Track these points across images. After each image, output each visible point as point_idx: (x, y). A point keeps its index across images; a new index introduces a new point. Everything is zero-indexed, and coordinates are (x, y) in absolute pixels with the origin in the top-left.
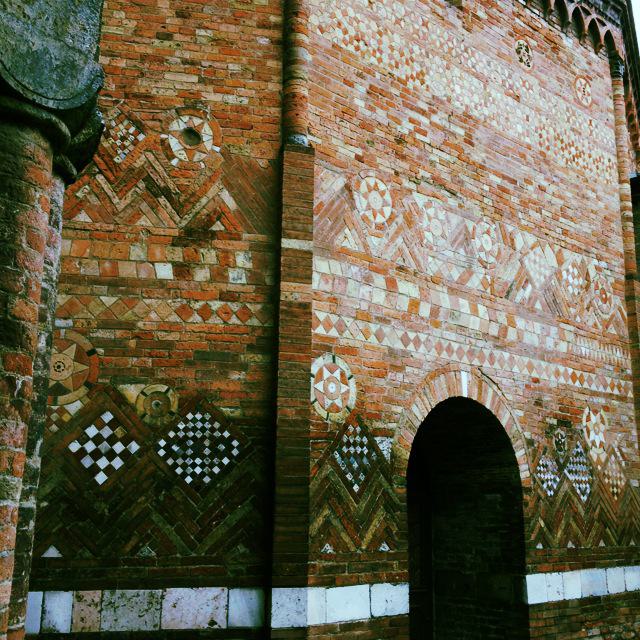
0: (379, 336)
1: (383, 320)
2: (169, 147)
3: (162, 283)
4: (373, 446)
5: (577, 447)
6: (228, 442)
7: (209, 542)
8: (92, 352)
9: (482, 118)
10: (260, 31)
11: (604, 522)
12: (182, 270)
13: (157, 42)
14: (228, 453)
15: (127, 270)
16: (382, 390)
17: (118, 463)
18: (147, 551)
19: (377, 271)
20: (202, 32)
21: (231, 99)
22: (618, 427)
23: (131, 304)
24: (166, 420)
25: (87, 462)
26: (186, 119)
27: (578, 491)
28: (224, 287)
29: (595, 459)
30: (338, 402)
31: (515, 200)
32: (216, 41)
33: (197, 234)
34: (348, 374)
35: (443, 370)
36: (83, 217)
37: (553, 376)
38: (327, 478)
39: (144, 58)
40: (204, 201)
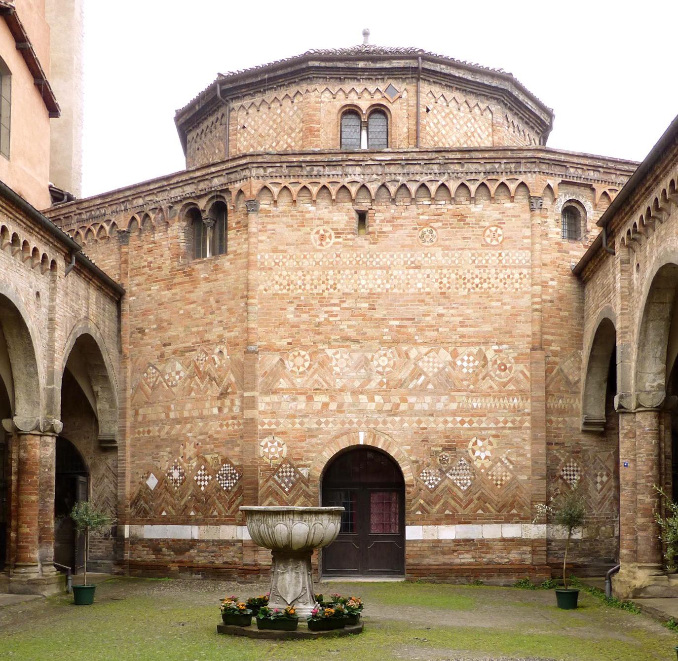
0: (301, 424)
1: (305, 416)
4: (296, 472)
5: (461, 461)
7: (231, 510)
9: (385, 291)
11: (483, 499)
12: (220, 410)
13: (210, 316)
15: (205, 412)
16: (303, 448)
17: (206, 483)
18: (215, 513)
19: (301, 394)
20: (223, 307)
21: (233, 334)
22: (509, 446)
23: (206, 424)
25: (199, 483)
26: (219, 347)
28: (233, 414)
29: (479, 465)
30: (277, 455)
31: (411, 330)
33: (223, 395)
34: (282, 443)
35: (347, 433)
36: (193, 394)
37: (437, 425)
38: (270, 486)
39: (207, 324)
40: (225, 380)
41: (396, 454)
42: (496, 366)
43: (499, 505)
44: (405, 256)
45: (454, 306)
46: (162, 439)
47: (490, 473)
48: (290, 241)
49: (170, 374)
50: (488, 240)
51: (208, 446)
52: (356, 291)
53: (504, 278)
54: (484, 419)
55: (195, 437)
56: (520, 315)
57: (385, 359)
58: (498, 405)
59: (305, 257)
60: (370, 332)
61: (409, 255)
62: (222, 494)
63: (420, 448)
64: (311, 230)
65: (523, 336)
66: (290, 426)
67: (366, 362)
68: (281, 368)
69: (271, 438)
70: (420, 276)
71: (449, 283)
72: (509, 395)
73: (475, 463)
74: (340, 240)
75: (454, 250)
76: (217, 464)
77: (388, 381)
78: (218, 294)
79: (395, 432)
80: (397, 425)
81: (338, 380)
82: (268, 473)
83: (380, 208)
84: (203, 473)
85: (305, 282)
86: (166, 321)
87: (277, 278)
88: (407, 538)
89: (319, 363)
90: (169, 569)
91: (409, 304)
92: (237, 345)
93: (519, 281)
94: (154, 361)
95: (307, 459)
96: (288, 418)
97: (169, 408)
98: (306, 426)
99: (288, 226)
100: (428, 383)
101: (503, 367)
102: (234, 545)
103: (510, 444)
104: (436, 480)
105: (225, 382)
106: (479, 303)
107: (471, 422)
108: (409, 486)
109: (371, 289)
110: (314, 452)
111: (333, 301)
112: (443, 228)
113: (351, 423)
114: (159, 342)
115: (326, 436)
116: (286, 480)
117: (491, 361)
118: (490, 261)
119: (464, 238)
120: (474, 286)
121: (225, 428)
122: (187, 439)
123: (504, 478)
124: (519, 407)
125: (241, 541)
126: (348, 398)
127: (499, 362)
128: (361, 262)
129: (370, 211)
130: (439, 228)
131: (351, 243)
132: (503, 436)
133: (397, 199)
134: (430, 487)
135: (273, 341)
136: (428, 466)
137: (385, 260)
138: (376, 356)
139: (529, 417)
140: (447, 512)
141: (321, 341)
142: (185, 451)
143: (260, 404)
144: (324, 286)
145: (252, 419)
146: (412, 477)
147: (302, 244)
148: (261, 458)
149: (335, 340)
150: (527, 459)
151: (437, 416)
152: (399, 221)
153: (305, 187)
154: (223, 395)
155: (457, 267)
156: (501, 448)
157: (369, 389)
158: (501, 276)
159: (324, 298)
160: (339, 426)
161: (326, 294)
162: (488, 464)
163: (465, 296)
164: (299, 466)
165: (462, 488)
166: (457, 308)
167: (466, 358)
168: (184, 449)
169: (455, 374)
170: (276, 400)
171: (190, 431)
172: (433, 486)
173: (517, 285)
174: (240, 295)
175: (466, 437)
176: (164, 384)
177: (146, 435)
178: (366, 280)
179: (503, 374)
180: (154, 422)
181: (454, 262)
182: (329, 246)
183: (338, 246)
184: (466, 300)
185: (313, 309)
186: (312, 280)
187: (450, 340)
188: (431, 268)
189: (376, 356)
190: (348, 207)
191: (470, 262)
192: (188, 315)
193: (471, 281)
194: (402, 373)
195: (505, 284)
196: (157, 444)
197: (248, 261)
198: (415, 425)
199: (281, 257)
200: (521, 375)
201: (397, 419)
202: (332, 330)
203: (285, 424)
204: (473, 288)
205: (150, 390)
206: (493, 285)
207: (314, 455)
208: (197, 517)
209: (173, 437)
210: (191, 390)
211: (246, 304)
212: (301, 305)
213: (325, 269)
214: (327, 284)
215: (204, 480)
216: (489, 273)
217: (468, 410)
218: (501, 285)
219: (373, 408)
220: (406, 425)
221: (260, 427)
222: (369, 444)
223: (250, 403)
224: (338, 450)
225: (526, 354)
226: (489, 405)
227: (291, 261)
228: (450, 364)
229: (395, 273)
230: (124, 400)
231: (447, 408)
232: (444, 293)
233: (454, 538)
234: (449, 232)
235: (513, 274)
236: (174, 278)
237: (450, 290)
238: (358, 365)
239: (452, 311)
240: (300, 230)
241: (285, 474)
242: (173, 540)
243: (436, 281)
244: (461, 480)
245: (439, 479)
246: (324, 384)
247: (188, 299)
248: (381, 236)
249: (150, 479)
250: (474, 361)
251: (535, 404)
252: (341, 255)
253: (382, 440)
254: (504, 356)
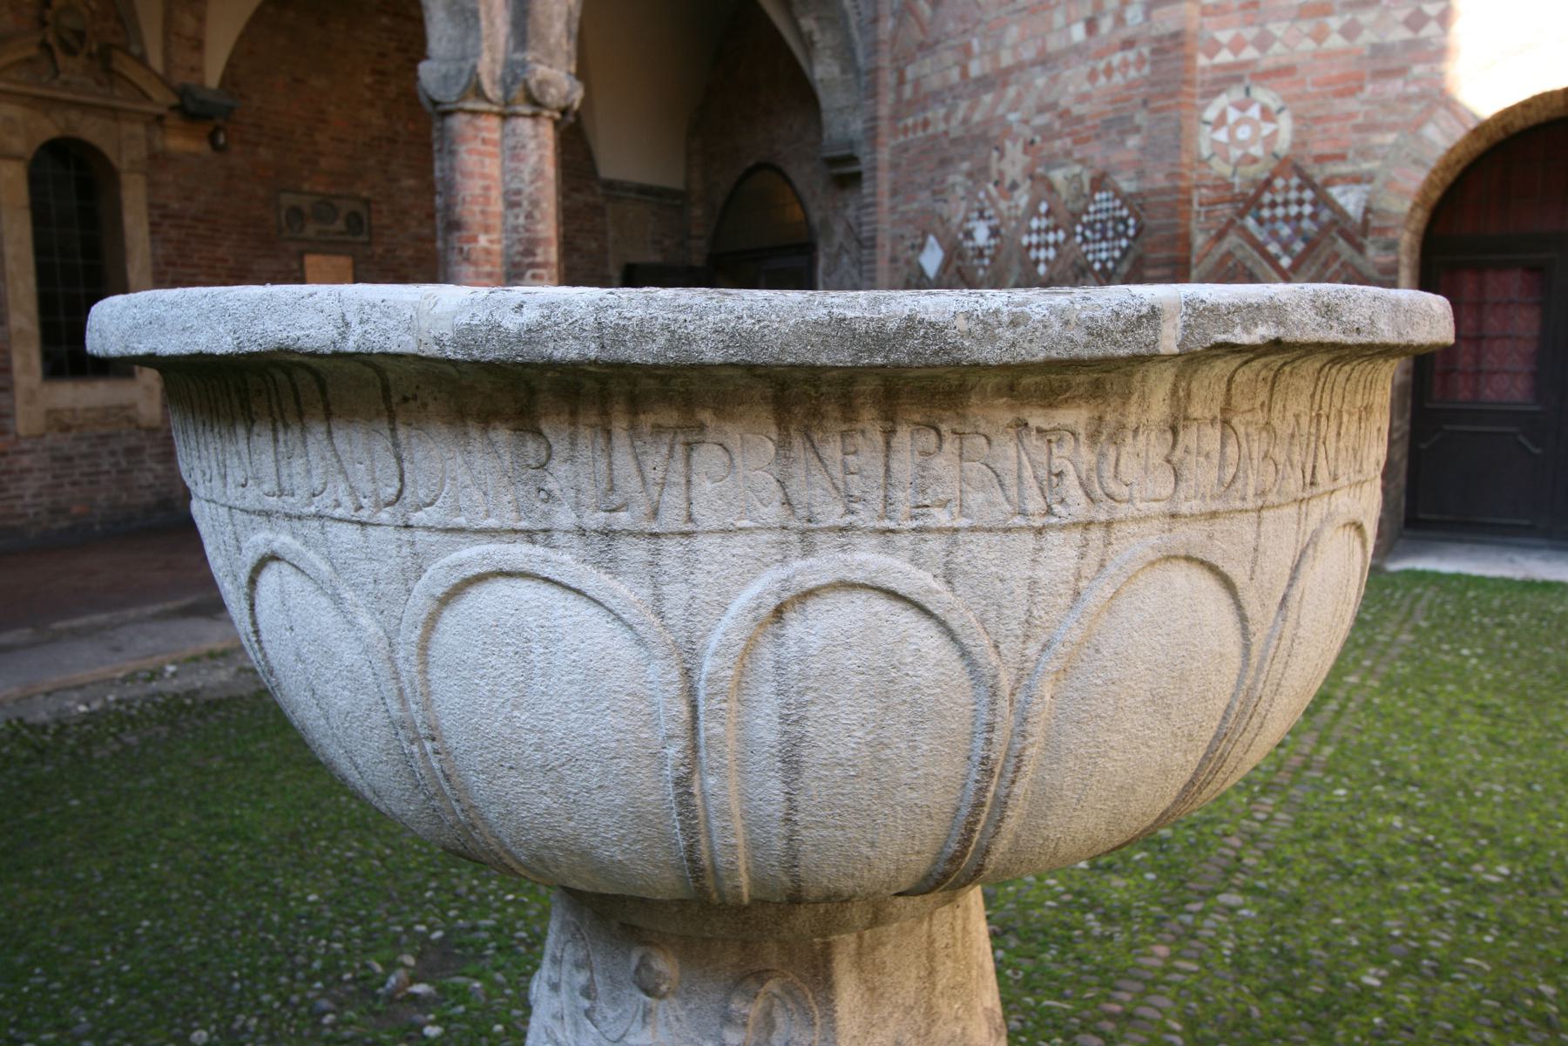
0: (1349, 32)
3: (1077, 50)
4: (1322, 200)
12: (1091, 26)
14: (1125, 234)
15: (1054, 44)
16: (1351, 116)
23: (1054, 79)
24: (1081, 204)
25: (1033, 254)
28: (1125, 33)
30: (1257, 150)
34: (1274, 106)
38: (1229, 254)
46: (955, 142)
51: (1058, 144)
66: (1308, 45)
69: (1237, 94)
76: (1079, 195)
82: (1226, 210)
84: (1044, 223)
95: (1364, 154)
97: (967, 51)
98: (1367, 38)
110: (1392, 127)
116: (1285, 231)
121: (1102, 80)
122: (1007, 130)
145: (1176, 35)
148: (1204, 162)
164: (1330, 181)
171: (1014, 108)
177: (920, 134)
180: (937, 96)
196: (940, 154)
207: (1390, 138)
209: (977, 132)
215: (1047, 245)
221: (1202, 61)
230: (874, 48)
241: (1280, 211)
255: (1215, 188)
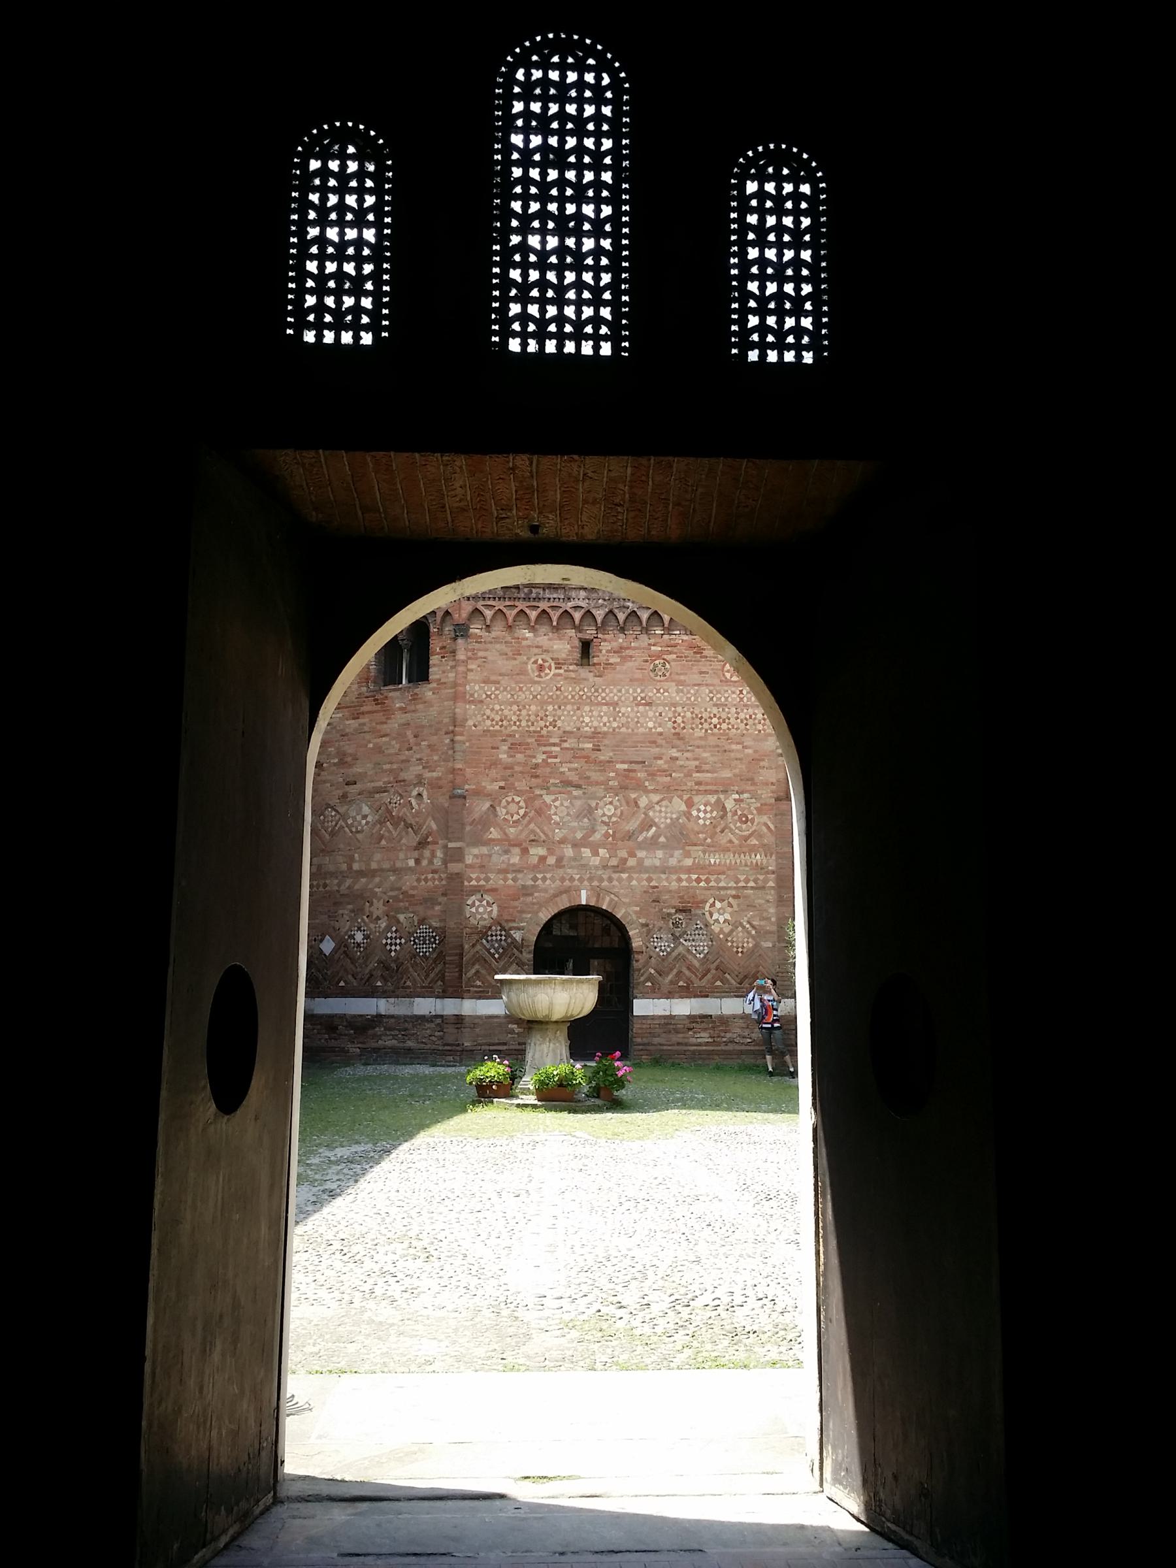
0: (514, 880)
1: (519, 871)
2: (411, 804)
3: (410, 868)
4: (508, 936)
5: (697, 924)
6: (434, 937)
8: (388, 902)
9: (611, 730)
10: (446, 736)
12: (418, 861)
13: (407, 752)
15: (399, 865)
17: (398, 948)
18: (409, 983)
19: (515, 845)
20: (423, 743)
21: (435, 774)
23: (400, 879)
24: (413, 929)
25: (388, 947)
26: (417, 789)
27: (694, 952)
28: (434, 868)
30: (485, 916)
32: (429, 746)
33: (422, 844)
35: (567, 891)
36: (383, 842)
37: (667, 882)
39: (403, 761)
40: (425, 827)
41: (624, 916)
42: (736, 817)
43: (741, 976)
44: (635, 691)
45: (690, 748)
47: (729, 939)
48: (503, 671)
49: (354, 818)
50: (728, 675)
51: (402, 904)
52: (579, 729)
53: (746, 719)
54: (722, 877)
55: (385, 893)
56: (763, 760)
57: (611, 807)
58: (738, 861)
59: (521, 689)
60: (595, 776)
61: (639, 691)
62: (418, 960)
63: (651, 910)
64: (529, 659)
65: (767, 784)
66: (501, 882)
67: (590, 811)
68: (492, 816)
70: (651, 714)
71: (683, 722)
72: (750, 852)
73: (713, 927)
74: (561, 671)
75: (689, 686)
76: (413, 925)
77: (614, 832)
78: (416, 727)
79: (622, 891)
80: (625, 883)
81: (557, 831)
82: (477, 937)
83: (606, 636)
84: (394, 935)
85: (521, 718)
86: (351, 755)
87: (488, 712)
88: (634, 1014)
89: (536, 810)
90: (348, 1051)
91: (639, 745)
92: (440, 787)
93: (762, 721)
94: (334, 801)
96: (498, 873)
97: (352, 858)
98: (520, 882)
99: (501, 654)
100: (659, 836)
101: (744, 819)
102: (432, 1022)
103: (751, 906)
104: (669, 946)
105: (424, 830)
106: (718, 746)
107: (707, 881)
108: (638, 953)
109: (595, 728)
110: (529, 913)
111: (552, 741)
112: (678, 661)
113: (572, 879)
114: (341, 780)
115: (542, 894)
116: (496, 945)
117: (731, 811)
118: (730, 699)
119: (701, 673)
120: (712, 726)
121: (423, 883)
123: (745, 945)
124: (762, 864)
125: (442, 1016)
126: (569, 852)
127: (739, 813)
128: (584, 697)
129: (595, 640)
130: (674, 660)
131: (573, 675)
132: (745, 897)
133: (626, 628)
134: (661, 954)
135: (483, 784)
136: (659, 930)
137: (611, 695)
138: (601, 804)
139: (773, 876)
140: (681, 983)
141: (537, 787)
142: (371, 909)
143: (467, 857)
144: (542, 723)
145: (457, 874)
146: (641, 943)
147: (518, 674)
149: (555, 785)
150: (772, 924)
151: (670, 873)
152: (627, 651)
153: (522, 610)
154: (422, 844)
155: (693, 705)
156: (742, 910)
157: (593, 841)
158: (742, 716)
159: (542, 736)
160: (558, 883)
161: (544, 732)
162: (727, 929)
163: (701, 738)
164: (511, 929)
165: (698, 955)
166: (693, 751)
167: (702, 808)
168: (370, 906)
169: (690, 825)
170: (486, 852)
172: (665, 953)
173: (760, 727)
174: (444, 730)
175: (703, 897)
176: (347, 829)
177: (321, 889)
178: (590, 717)
179: (744, 826)
180: (332, 875)
181: (690, 698)
182: (548, 678)
183: (559, 678)
184: (703, 743)
185: (530, 749)
186: (529, 715)
187: (684, 788)
188: (665, 705)
189: (601, 804)
190: (570, 635)
191: (708, 699)
192: (379, 750)
193: (709, 720)
194: (630, 824)
195: (746, 724)
197: (455, 692)
198: (645, 883)
199: (493, 689)
200: (764, 828)
201: (625, 876)
202: (550, 773)
203: (495, 880)
204: (711, 729)
205: (327, 836)
206: (733, 726)
207: (529, 916)
208: (385, 988)
210: (381, 837)
211: (452, 740)
212: (516, 744)
213: (543, 703)
214: (546, 721)
215: (396, 944)
216: (729, 713)
217: (703, 867)
218: (742, 726)
219: (597, 863)
220: (634, 883)
221: (466, 883)
222: (592, 904)
223: (457, 856)
224: (556, 912)
225: (770, 805)
226: (728, 861)
227: (505, 693)
228: (685, 815)
229: (623, 710)
231: (681, 864)
232: (678, 734)
233: (688, 1014)
234: (684, 665)
235: (756, 714)
236: (362, 706)
237: (685, 731)
238: (580, 814)
239: (686, 755)
240: (515, 659)
241: (494, 938)
242: (354, 1016)
243: (670, 719)
244: (698, 947)
245: (672, 945)
246: (541, 834)
247: (379, 731)
248: (607, 668)
249: (325, 942)
250: (711, 812)
251: (780, 861)
252: (562, 689)
253: (608, 899)
254: (745, 805)
255: (471, 928)
